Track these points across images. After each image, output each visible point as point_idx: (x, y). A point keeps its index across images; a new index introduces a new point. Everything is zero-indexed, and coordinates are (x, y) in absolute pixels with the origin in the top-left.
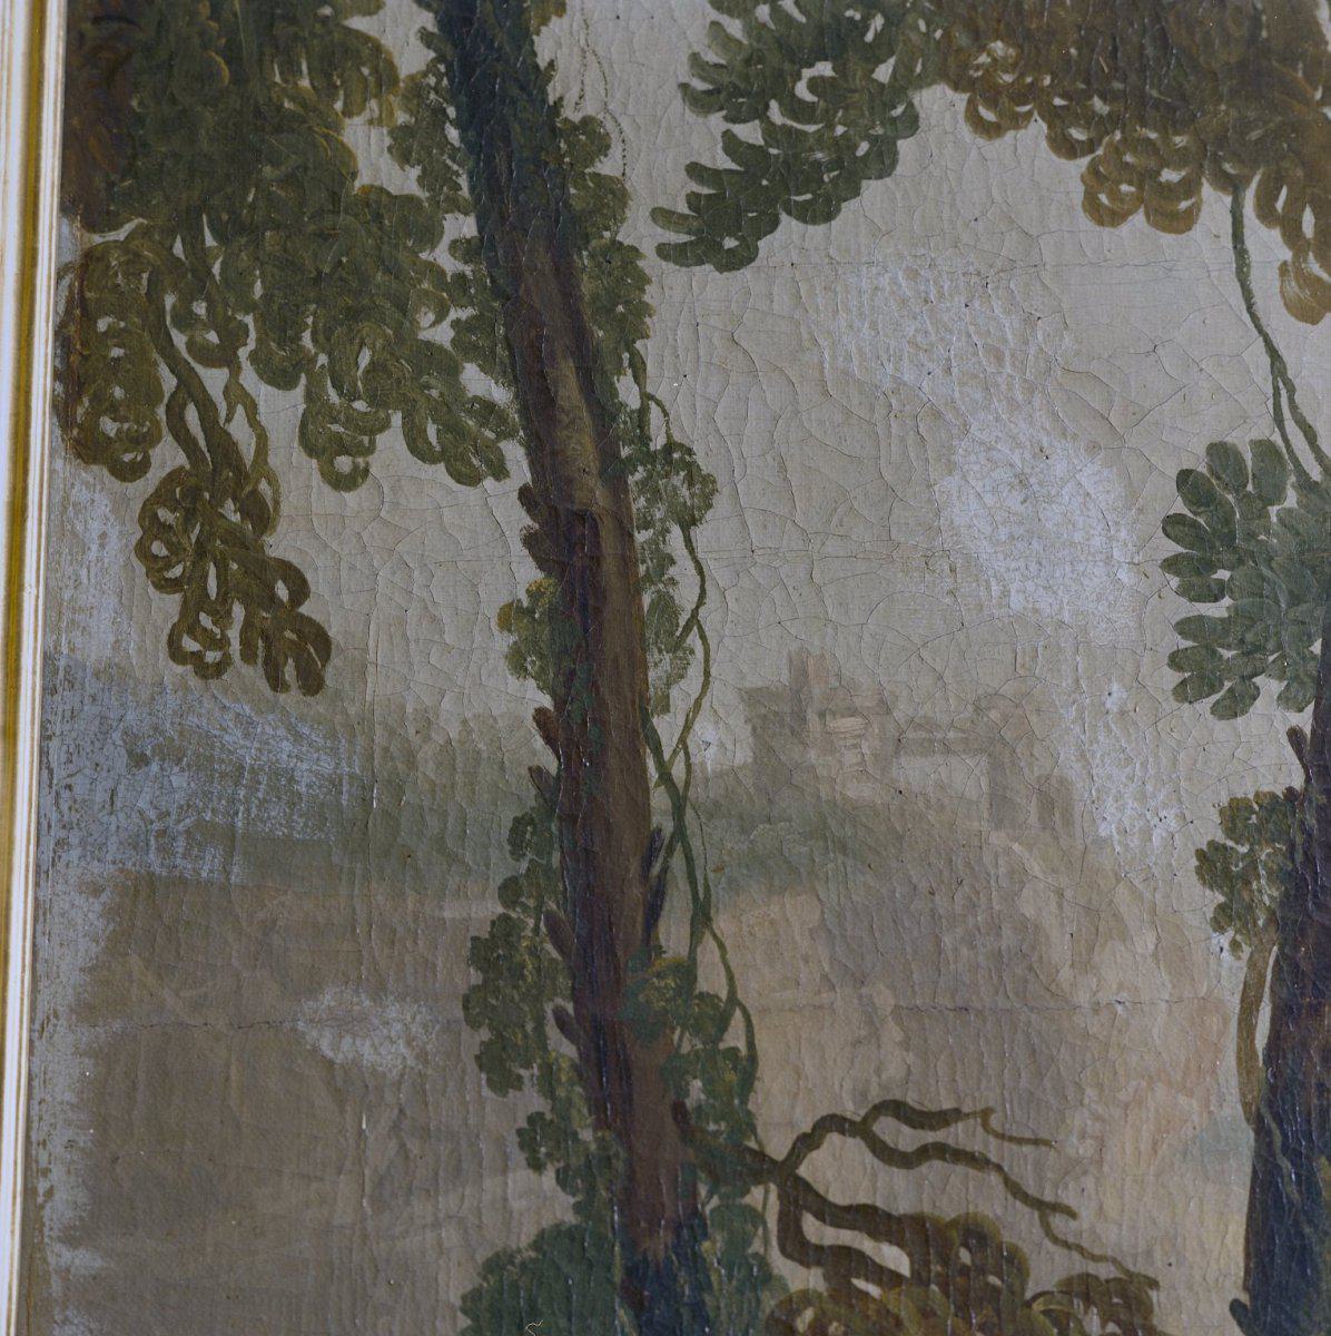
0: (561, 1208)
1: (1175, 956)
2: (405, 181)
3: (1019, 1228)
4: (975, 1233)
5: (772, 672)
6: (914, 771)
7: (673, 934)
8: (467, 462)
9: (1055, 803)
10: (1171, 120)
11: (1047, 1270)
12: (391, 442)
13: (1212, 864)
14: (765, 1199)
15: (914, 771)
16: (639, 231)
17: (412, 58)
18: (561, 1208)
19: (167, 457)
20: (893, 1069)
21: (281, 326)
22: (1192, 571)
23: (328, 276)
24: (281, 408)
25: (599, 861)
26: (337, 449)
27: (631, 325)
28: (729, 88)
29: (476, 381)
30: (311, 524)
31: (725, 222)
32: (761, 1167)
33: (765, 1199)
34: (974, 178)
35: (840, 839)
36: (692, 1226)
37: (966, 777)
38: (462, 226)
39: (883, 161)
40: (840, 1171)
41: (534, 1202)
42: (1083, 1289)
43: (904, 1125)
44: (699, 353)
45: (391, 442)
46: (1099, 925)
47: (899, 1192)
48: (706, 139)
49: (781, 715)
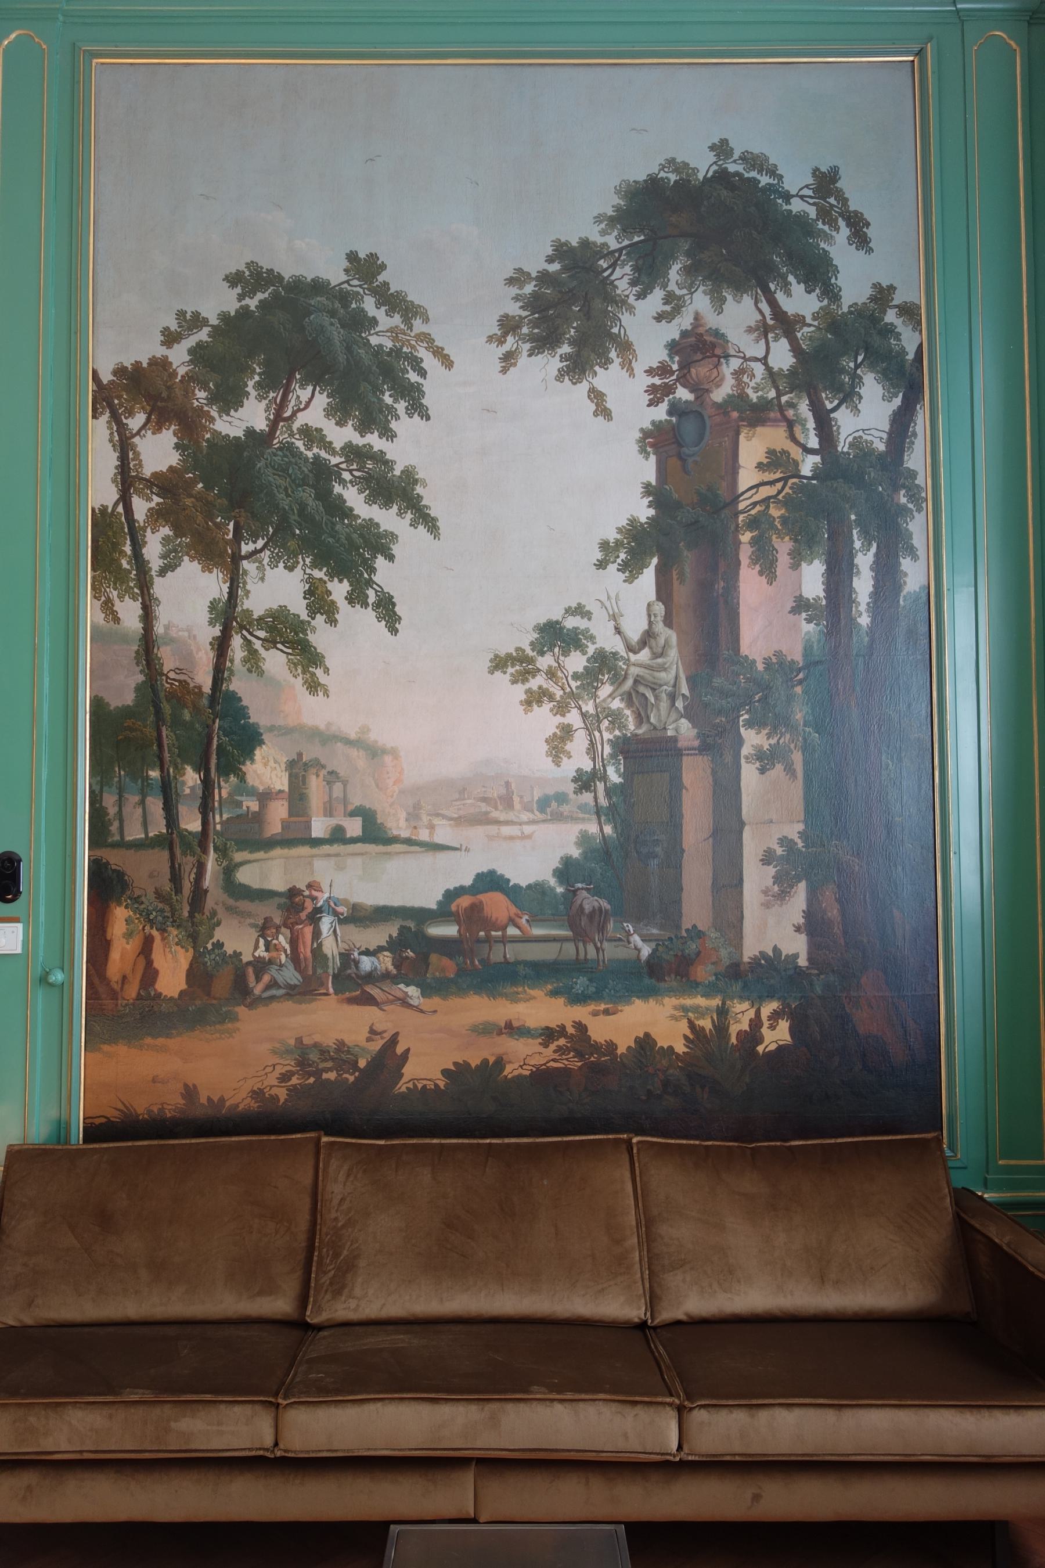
0: (144, 679)
1: (206, 653)
2: (128, 567)
3: (189, 681)
4: (185, 681)
5: (166, 623)
6: (180, 633)
7: (155, 650)
8: (135, 599)
9: (195, 637)
10: (211, 560)
11: (192, 685)
12: (127, 597)
13: (211, 643)
14: (164, 678)
15: (180, 633)
16: (153, 573)
17: (129, 552)
18: (144, 679)
19: (103, 598)
20: (178, 665)
21: (115, 584)
22: (211, 612)
23: (120, 578)
24: (115, 593)
25: (148, 641)
26: (121, 597)
27: (152, 584)
28: (163, 557)
29: (136, 590)
30: (118, 606)
31: (163, 572)
32: (164, 675)
33: (164, 678)
34: (189, 567)
35: (172, 640)
36: (156, 681)
37: (186, 634)
38: (134, 572)
39: (180, 565)
40: (172, 675)
41: (141, 678)
42: (195, 687)
43: (178, 670)
44: (160, 587)
45: (127, 597)
46: (199, 650)
47: (177, 677)
48: (161, 562)
49: (167, 627)
